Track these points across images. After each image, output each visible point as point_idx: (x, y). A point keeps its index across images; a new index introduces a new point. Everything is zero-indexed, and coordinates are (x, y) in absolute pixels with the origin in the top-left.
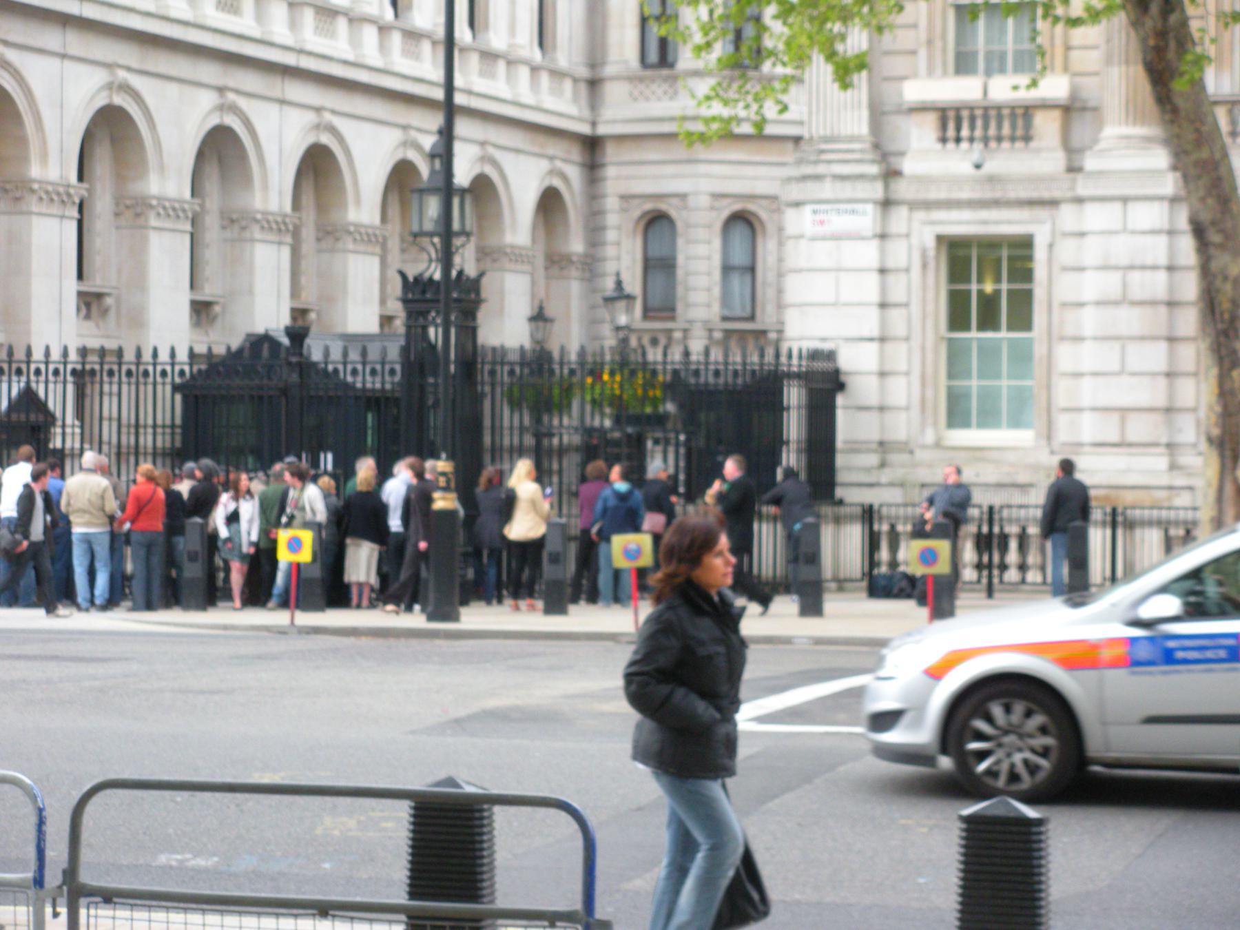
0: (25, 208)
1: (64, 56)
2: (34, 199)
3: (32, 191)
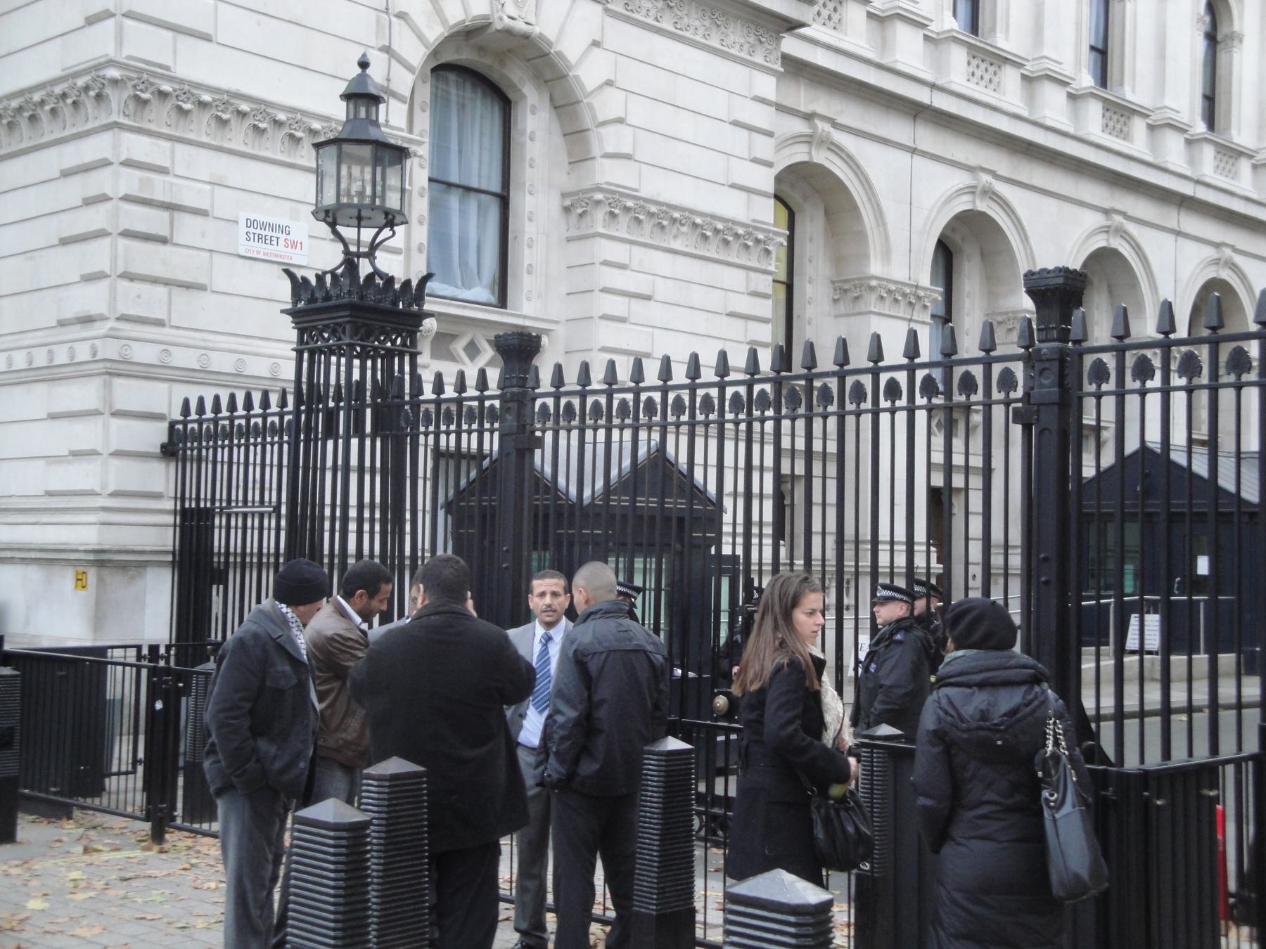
0: (863, 309)
1: (913, 151)
2: (873, 297)
3: (872, 289)
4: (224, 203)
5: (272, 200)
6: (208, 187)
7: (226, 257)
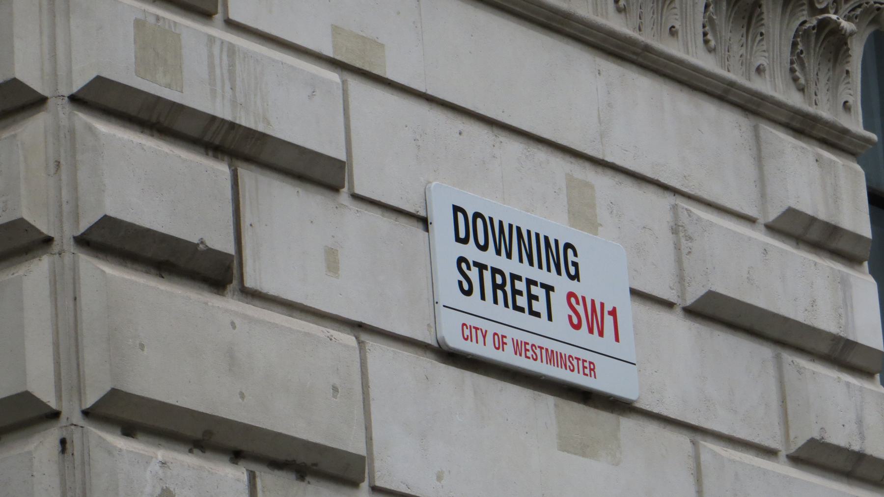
4: (385, 144)
5: (514, 147)
6: (333, 76)
7: (407, 355)
